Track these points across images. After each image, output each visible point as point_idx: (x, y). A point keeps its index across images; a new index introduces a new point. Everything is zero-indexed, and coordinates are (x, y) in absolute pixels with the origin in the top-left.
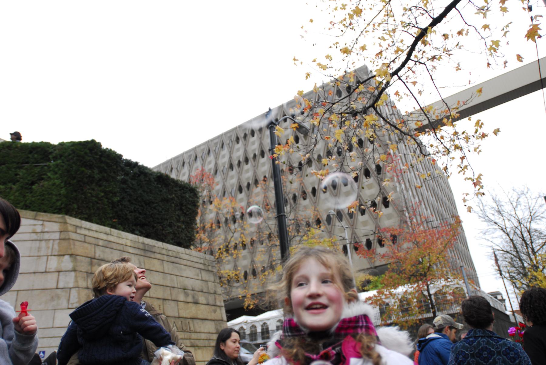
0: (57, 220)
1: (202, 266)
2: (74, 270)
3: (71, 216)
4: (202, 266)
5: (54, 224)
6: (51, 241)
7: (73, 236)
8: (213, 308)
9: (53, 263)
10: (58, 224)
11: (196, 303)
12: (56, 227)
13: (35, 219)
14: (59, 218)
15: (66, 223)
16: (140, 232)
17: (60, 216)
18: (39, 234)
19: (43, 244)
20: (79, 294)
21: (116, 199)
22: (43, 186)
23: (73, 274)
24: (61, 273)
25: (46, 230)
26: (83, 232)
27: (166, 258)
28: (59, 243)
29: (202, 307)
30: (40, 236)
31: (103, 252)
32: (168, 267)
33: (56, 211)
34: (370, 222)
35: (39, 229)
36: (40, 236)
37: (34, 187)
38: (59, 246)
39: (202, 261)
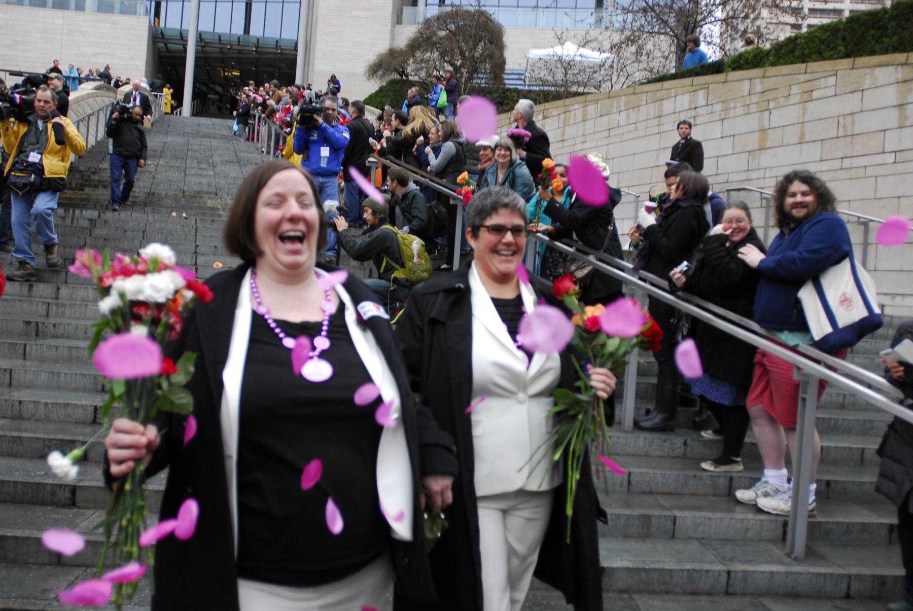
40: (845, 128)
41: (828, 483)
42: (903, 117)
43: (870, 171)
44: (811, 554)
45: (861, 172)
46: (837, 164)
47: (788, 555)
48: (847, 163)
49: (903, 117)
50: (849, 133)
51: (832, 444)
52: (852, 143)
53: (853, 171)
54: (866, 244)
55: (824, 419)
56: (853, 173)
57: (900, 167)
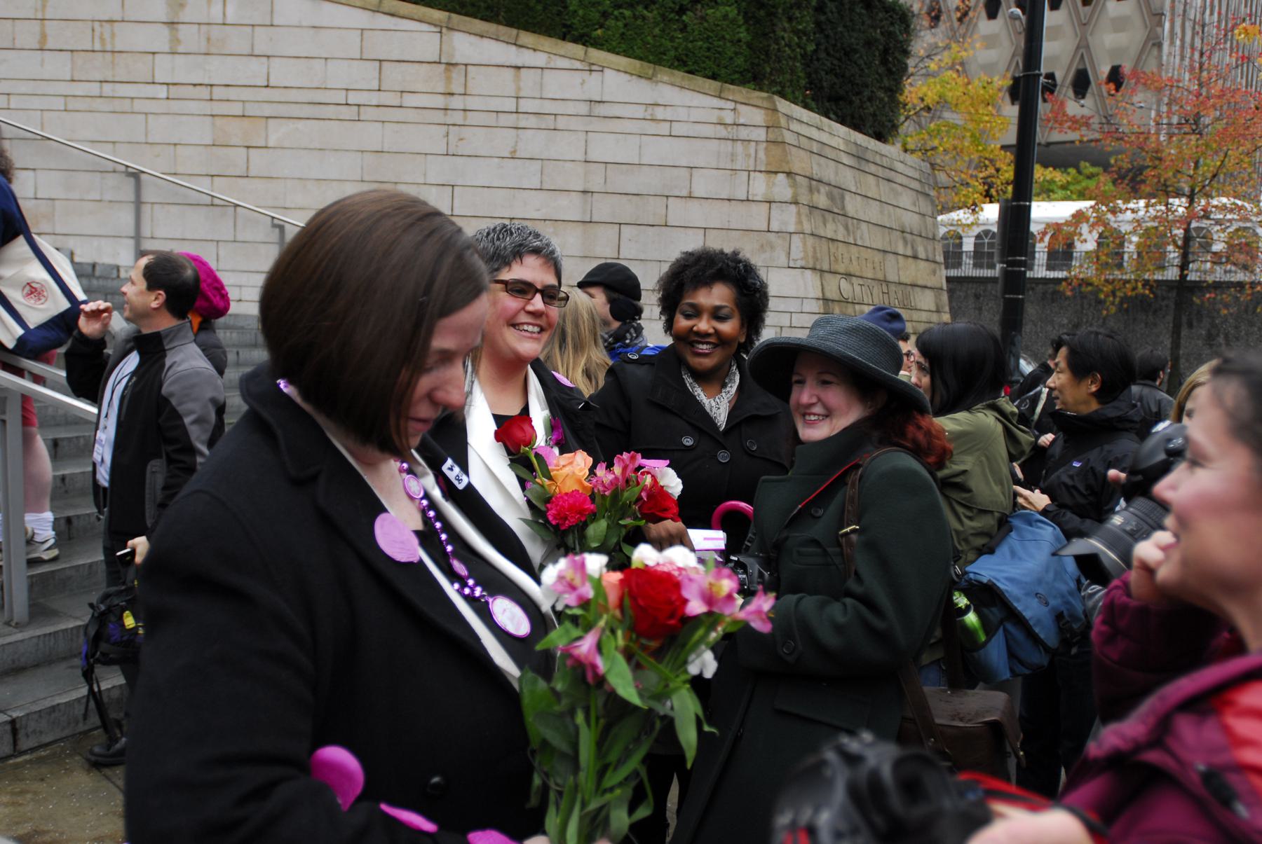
0: (759, 103)
1: (915, 185)
2: (796, 203)
3: (783, 95)
4: (915, 185)
5: (754, 110)
6: (753, 144)
7: (789, 138)
8: (933, 265)
9: (760, 186)
10: (763, 112)
11: (915, 257)
12: (758, 116)
13: (720, 97)
14: (763, 98)
15: (775, 110)
16: (835, 114)
17: (765, 95)
18: (729, 128)
19: (739, 147)
20: (805, 244)
21: (811, 47)
22: (703, 18)
23: (793, 208)
24: (773, 205)
25: (742, 121)
26: (795, 126)
27: (880, 172)
28: (766, 149)
29: (922, 264)
30: (732, 132)
31: (819, 165)
32: (884, 191)
33: (737, 76)
34: (1068, 30)
35: (729, 118)
36: (732, 132)
37: (684, 17)
38: (766, 154)
39: (917, 175)
40: (102, 40)
41: (69, 520)
42: (175, 40)
43: (138, 105)
44: (38, 612)
45: (126, 105)
46: (94, 89)
47: (8, 624)
48: (107, 89)
49: (175, 40)
50: (109, 48)
51: (78, 470)
52: (113, 62)
53: (117, 102)
54: (138, 203)
55: (69, 439)
56: (117, 105)
57: (175, 106)
